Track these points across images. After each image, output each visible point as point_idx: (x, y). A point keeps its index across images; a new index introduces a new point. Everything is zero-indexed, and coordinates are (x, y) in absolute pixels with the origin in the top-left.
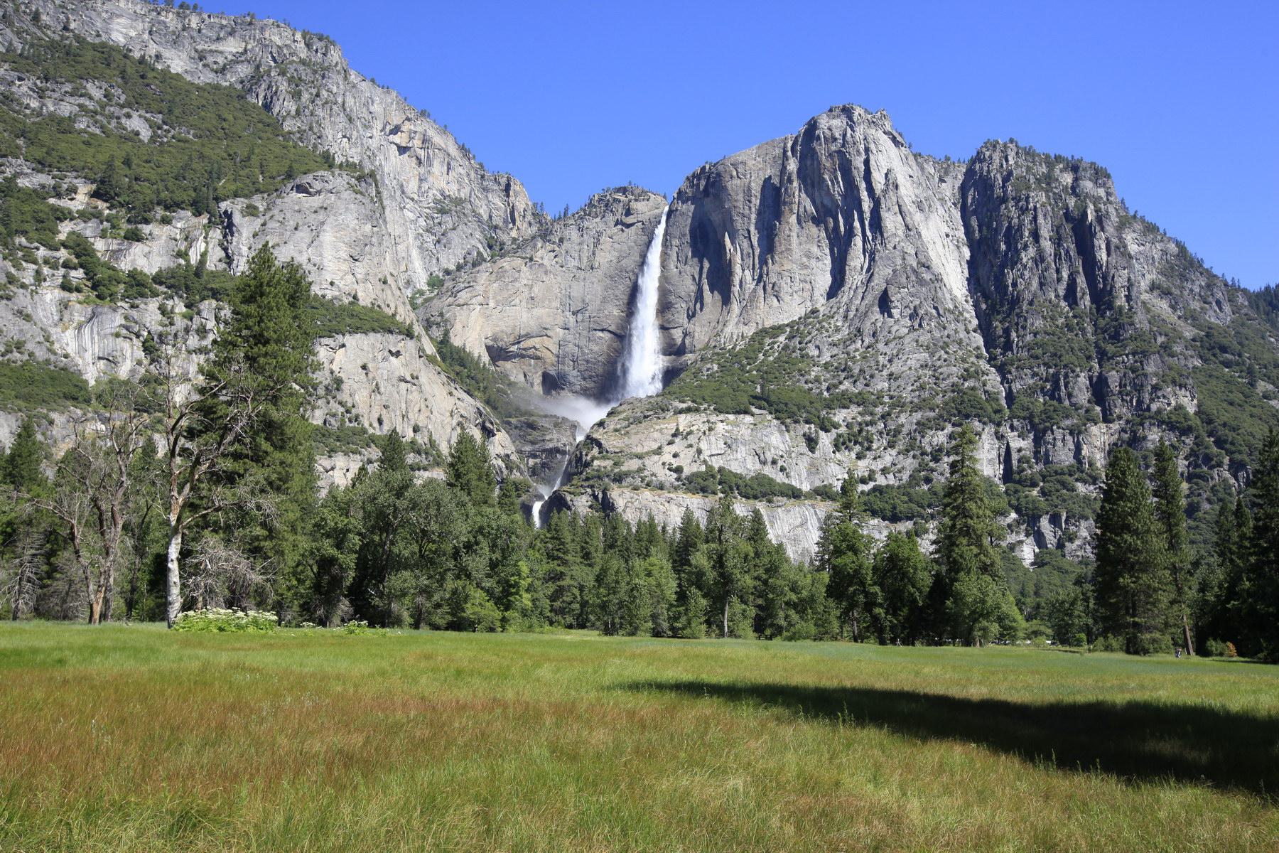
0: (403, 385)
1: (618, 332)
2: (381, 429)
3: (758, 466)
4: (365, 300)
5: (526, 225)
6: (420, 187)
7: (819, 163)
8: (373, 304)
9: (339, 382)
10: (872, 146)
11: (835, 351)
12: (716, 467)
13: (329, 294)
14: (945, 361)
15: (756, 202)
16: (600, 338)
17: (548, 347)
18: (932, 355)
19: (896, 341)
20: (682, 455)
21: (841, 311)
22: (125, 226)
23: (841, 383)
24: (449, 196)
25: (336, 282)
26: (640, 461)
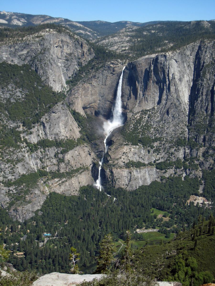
0: (78, 156)
1: (112, 102)
5: (87, 56)
6: (61, 54)
7: (158, 69)
9: (69, 161)
10: (170, 67)
15: (143, 74)
16: (108, 103)
17: (95, 105)
18: (175, 128)
23: (156, 134)
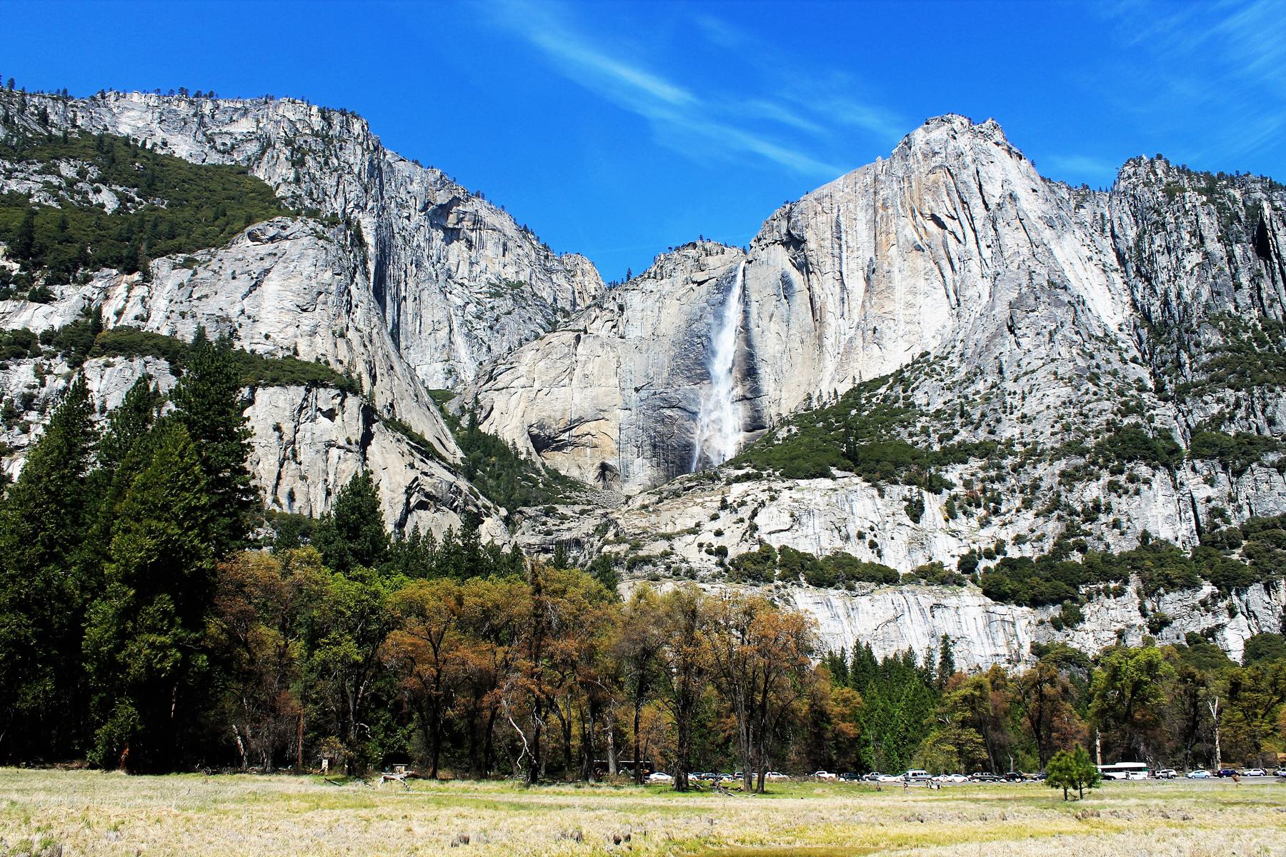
2: (290, 507)
3: (838, 544)
6: (471, 271)
10: (982, 157)
11: (949, 396)
12: (776, 546)
13: (260, 349)
14: (1095, 394)
18: (1077, 388)
20: (727, 533)
21: (956, 350)
23: (956, 432)
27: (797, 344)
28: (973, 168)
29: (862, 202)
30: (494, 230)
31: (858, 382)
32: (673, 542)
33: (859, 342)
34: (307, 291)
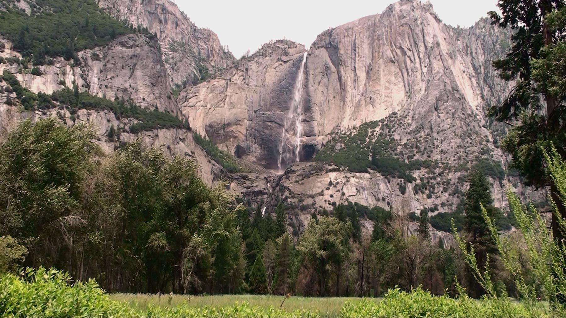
3: (375, 202)
4: (161, 109)
8: (165, 111)
10: (425, 22)
13: (143, 105)
14: (471, 143)
19: (443, 132)
20: (335, 196)
21: (410, 114)
22: (31, 67)
23: (414, 155)
24: (177, 41)
25: (146, 99)
26: (313, 200)
27: (332, 98)
28: (421, 27)
29: (367, 34)
30: (171, 14)
31: (364, 122)
32: (315, 199)
33: (363, 102)
34: (154, 76)
